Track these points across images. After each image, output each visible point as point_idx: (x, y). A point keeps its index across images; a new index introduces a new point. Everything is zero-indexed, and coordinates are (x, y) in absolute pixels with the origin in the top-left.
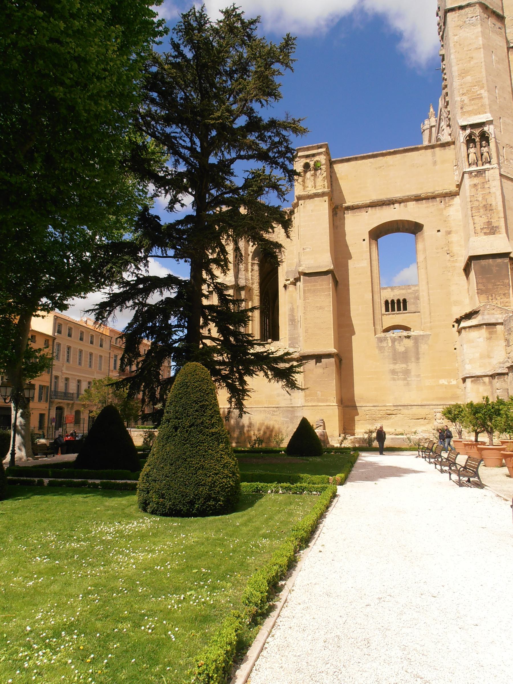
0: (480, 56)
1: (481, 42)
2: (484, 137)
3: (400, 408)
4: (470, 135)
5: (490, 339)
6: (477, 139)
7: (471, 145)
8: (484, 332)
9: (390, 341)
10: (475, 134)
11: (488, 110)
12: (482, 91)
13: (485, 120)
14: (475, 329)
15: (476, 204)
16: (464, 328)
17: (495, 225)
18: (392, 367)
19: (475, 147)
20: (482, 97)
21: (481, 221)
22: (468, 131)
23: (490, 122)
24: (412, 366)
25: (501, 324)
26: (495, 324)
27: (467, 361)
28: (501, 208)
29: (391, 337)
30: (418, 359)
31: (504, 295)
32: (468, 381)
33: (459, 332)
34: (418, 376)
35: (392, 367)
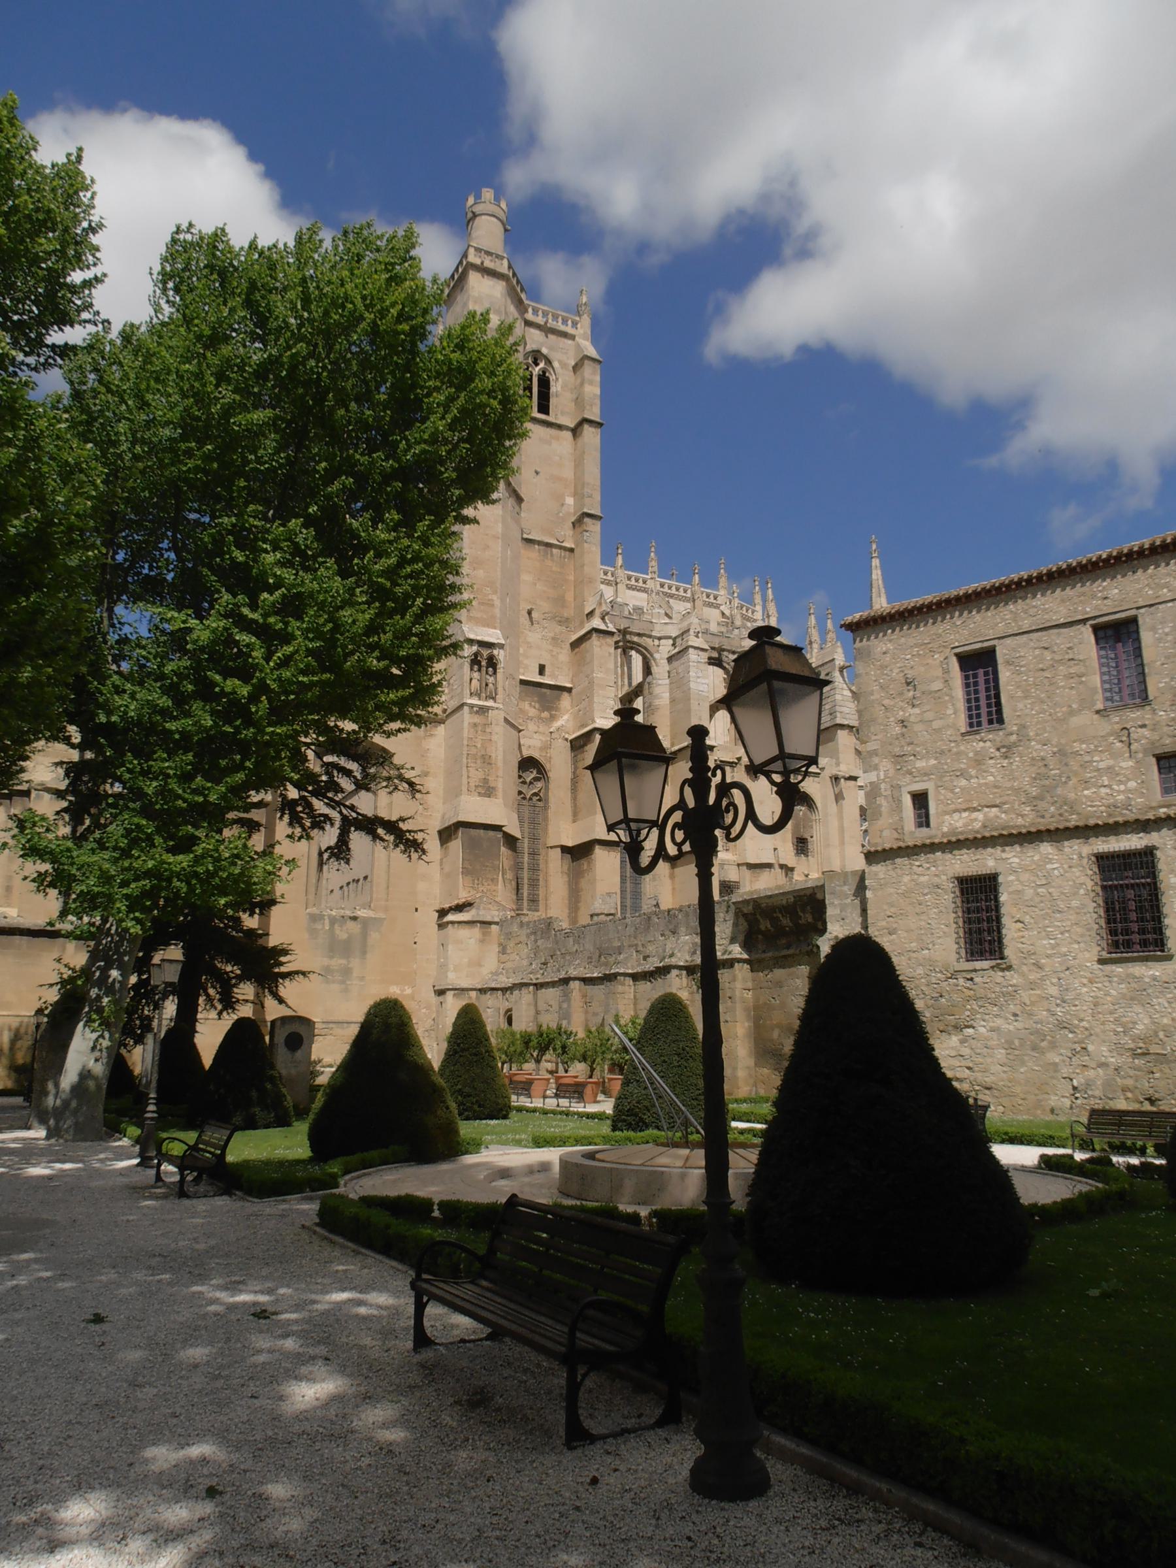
0: (498, 546)
1: (500, 531)
2: (492, 663)
3: (331, 1025)
4: (476, 654)
5: (482, 941)
6: (484, 663)
7: (476, 667)
8: (476, 931)
9: (327, 921)
10: (482, 656)
11: (498, 625)
12: (495, 597)
13: (495, 641)
14: (467, 926)
15: (473, 751)
16: (452, 923)
17: (492, 785)
18: (326, 961)
19: (479, 670)
20: (493, 605)
21: (476, 775)
22: (475, 648)
23: (501, 646)
24: (355, 963)
25: (497, 923)
26: (490, 923)
27: (451, 967)
28: (500, 764)
29: (329, 916)
30: (364, 952)
31: (492, 880)
32: (450, 994)
33: (441, 926)
34: (362, 978)
35: (326, 961)
